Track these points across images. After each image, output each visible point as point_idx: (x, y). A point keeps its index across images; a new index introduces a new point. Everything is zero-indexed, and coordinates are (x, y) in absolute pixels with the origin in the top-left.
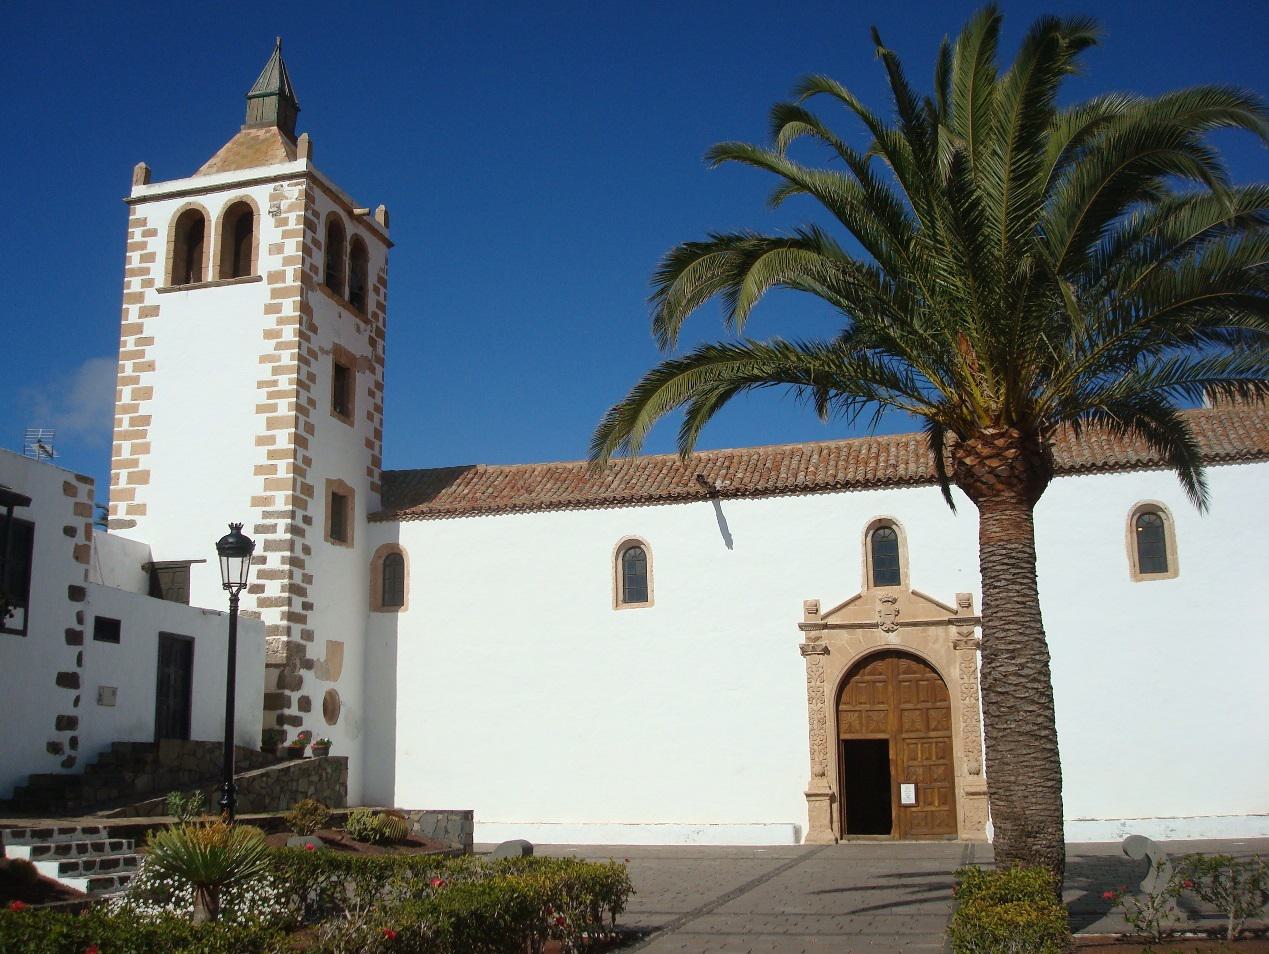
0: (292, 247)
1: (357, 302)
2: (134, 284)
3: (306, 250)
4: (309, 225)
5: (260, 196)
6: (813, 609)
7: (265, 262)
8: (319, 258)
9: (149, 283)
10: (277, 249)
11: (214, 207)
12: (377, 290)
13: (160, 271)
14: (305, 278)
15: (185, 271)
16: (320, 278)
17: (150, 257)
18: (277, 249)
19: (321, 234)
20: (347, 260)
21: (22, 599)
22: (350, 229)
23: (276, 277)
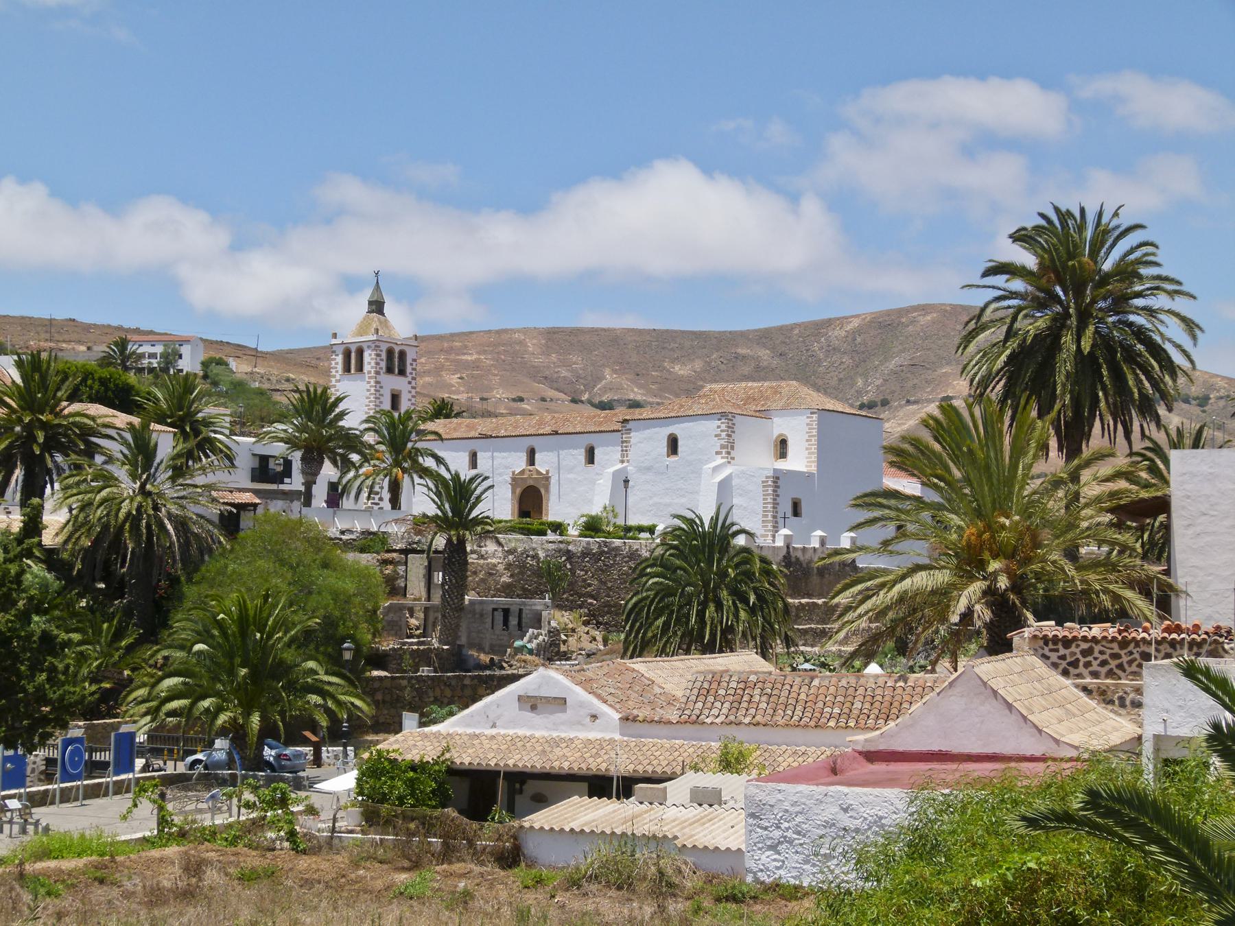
0: (373, 364)
1: (402, 372)
2: (333, 372)
3: (377, 364)
4: (378, 355)
5: (365, 346)
6: (513, 473)
7: (366, 368)
8: (383, 364)
9: (337, 372)
10: (369, 363)
11: (353, 349)
12: (411, 364)
13: (340, 367)
14: (377, 373)
15: (347, 369)
16: (384, 369)
17: (337, 363)
18: (369, 363)
19: (384, 356)
20: (396, 360)
21: (290, 476)
22: (397, 349)
23: (369, 372)
